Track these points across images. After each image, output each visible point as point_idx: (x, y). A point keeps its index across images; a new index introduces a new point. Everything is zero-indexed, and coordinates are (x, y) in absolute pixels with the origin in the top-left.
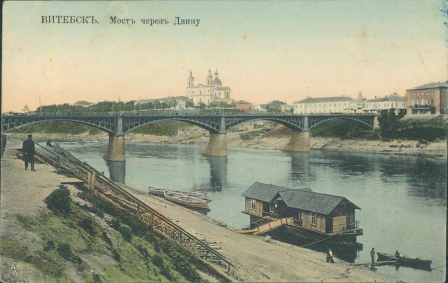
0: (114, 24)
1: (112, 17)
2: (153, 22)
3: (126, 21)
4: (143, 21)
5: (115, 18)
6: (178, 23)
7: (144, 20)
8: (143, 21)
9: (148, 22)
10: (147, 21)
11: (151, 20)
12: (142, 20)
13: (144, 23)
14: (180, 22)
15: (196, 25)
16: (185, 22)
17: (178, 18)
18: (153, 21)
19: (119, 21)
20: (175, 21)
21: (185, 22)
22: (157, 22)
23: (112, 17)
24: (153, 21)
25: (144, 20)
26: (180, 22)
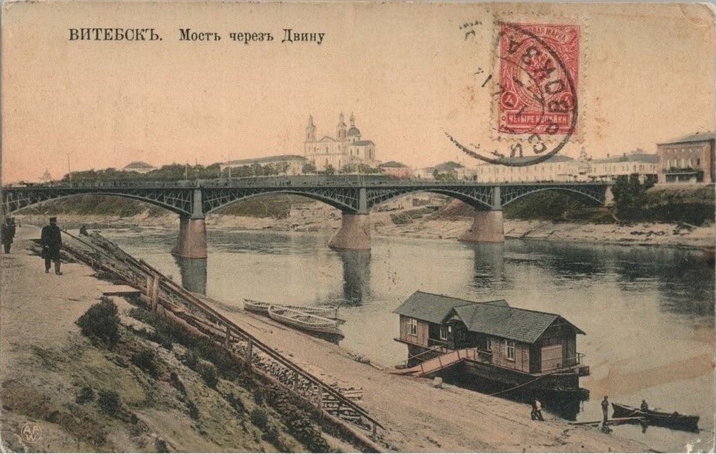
0: (185, 41)
1: (182, 30)
2: (249, 37)
3: (206, 37)
4: (233, 36)
5: (188, 30)
6: (289, 39)
7: (235, 34)
8: (233, 36)
9: (241, 38)
10: (238, 36)
11: (246, 34)
12: (231, 34)
13: (235, 40)
14: (292, 38)
15: (318, 43)
16: (300, 37)
17: (289, 31)
18: (248, 35)
19: (194, 37)
20: (283, 35)
21: (300, 37)
22: (255, 38)
23: (182, 30)
24: (248, 35)
25: (235, 34)
26: (292, 38)
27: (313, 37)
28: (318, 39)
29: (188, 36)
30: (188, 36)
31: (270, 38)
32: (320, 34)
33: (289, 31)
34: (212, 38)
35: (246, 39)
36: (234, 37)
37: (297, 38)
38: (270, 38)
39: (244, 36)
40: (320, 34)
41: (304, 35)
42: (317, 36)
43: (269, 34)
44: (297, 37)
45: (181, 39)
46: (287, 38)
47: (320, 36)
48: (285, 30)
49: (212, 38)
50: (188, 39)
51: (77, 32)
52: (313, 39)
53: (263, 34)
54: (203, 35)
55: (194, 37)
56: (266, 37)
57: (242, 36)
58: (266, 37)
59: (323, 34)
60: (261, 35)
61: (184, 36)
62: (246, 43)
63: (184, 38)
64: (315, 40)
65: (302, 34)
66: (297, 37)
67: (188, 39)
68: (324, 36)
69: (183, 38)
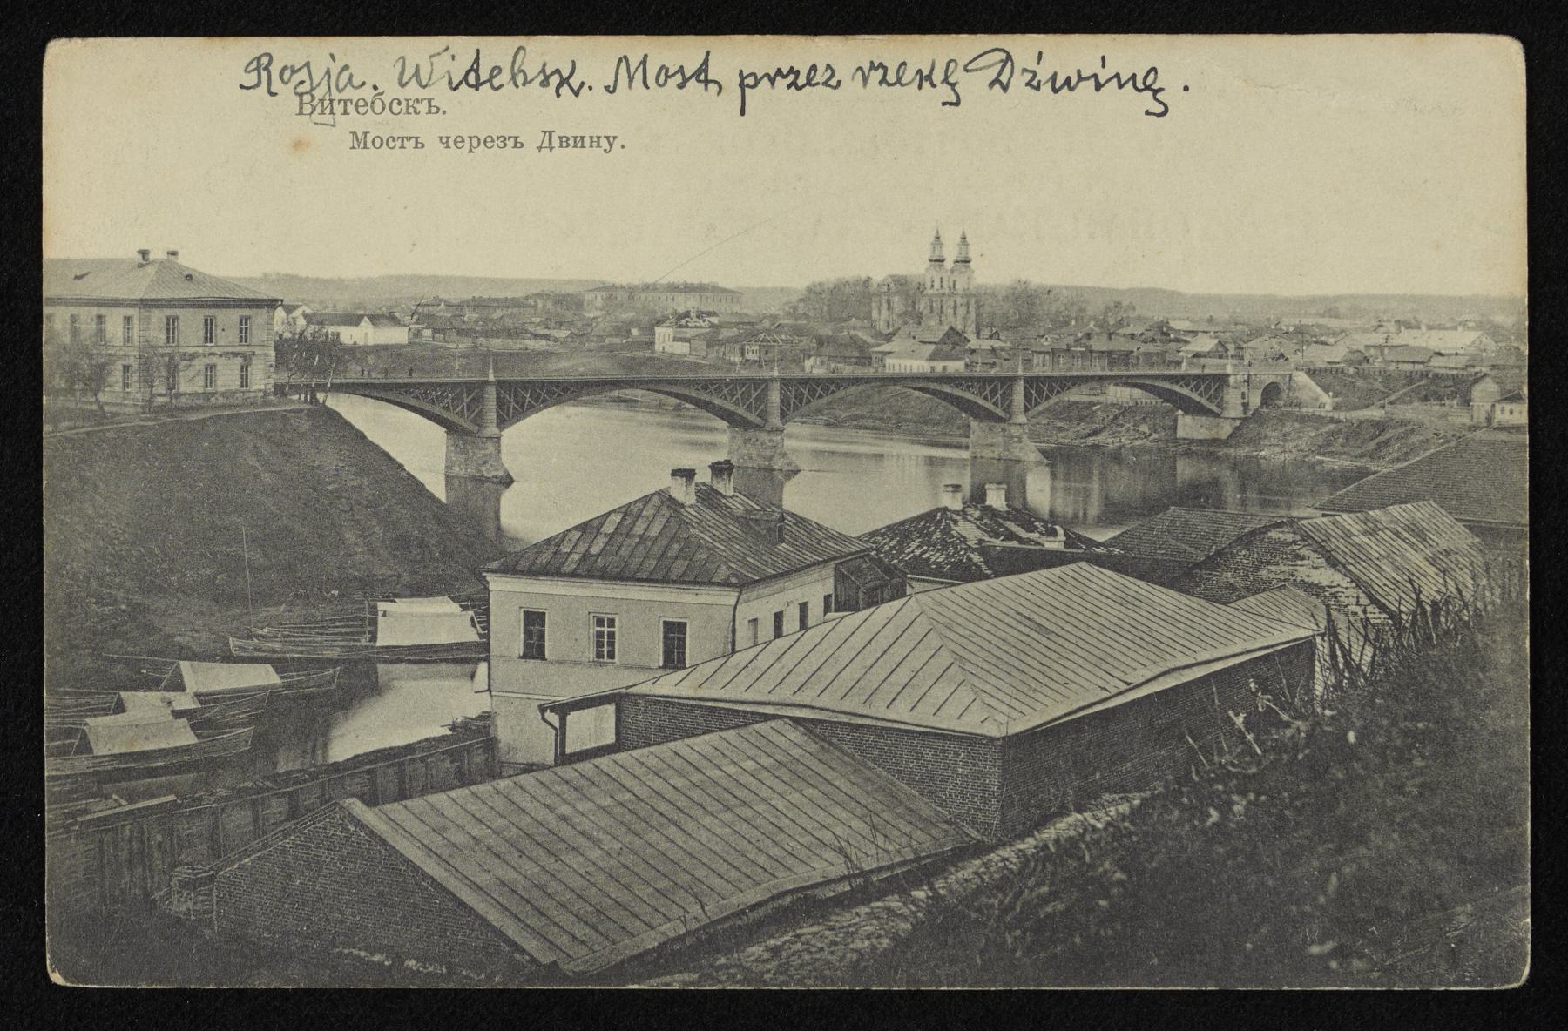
1: (354, 134)
3: (399, 143)
4: (445, 141)
5: (365, 134)
8: (445, 141)
11: (471, 138)
12: (441, 138)
14: (556, 142)
16: (571, 142)
17: (550, 133)
19: (378, 142)
23: (354, 134)
27: (595, 141)
28: (604, 143)
29: (365, 144)
30: (365, 144)
31: (518, 144)
33: (550, 133)
34: (410, 144)
35: (471, 145)
36: (447, 142)
37: (565, 144)
38: (518, 144)
39: (467, 140)
40: (607, 138)
41: (578, 139)
42: (604, 143)
43: (516, 138)
44: (564, 141)
45: (353, 148)
46: (546, 143)
47: (609, 141)
48: (545, 132)
49: (410, 144)
50: (365, 147)
52: (595, 144)
53: (505, 138)
54: (394, 140)
55: (378, 142)
56: (510, 143)
57: (463, 141)
58: (510, 143)
59: (615, 138)
60: (502, 139)
62: (471, 151)
64: (598, 146)
65: (575, 138)
66: (564, 141)
67: (365, 147)
68: (616, 140)
69: (356, 146)
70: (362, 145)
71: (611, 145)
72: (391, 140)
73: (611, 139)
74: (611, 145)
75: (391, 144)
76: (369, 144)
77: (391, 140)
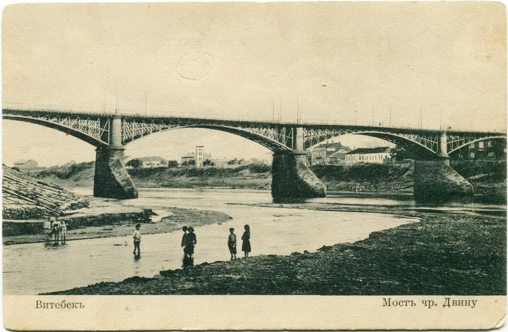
0: (387, 307)
15: (472, 307)
19: (395, 303)
24: (431, 303)
29: (389, 304)
30: (389, 304)
32: (473, 301)
35: (429, 305)
42: (471, 303)
45: (384, 306)
47: (473, 302)
50: (389, 305)
51: (456, 302)
54: (402, 302)
55: (395, 303)
61: (386, 304)
62: (429, 308)
63: (386, 304)
64: (469, 305)
69: (385, 305)
70: (388, 304)
71: (474, 305)
72: (401, 302)
73: (474, 302)
74: (474, 305)
75: (401, 304)
76: (391, 304)
77: (401, 302)
